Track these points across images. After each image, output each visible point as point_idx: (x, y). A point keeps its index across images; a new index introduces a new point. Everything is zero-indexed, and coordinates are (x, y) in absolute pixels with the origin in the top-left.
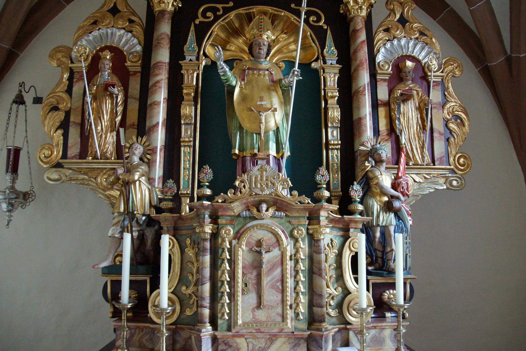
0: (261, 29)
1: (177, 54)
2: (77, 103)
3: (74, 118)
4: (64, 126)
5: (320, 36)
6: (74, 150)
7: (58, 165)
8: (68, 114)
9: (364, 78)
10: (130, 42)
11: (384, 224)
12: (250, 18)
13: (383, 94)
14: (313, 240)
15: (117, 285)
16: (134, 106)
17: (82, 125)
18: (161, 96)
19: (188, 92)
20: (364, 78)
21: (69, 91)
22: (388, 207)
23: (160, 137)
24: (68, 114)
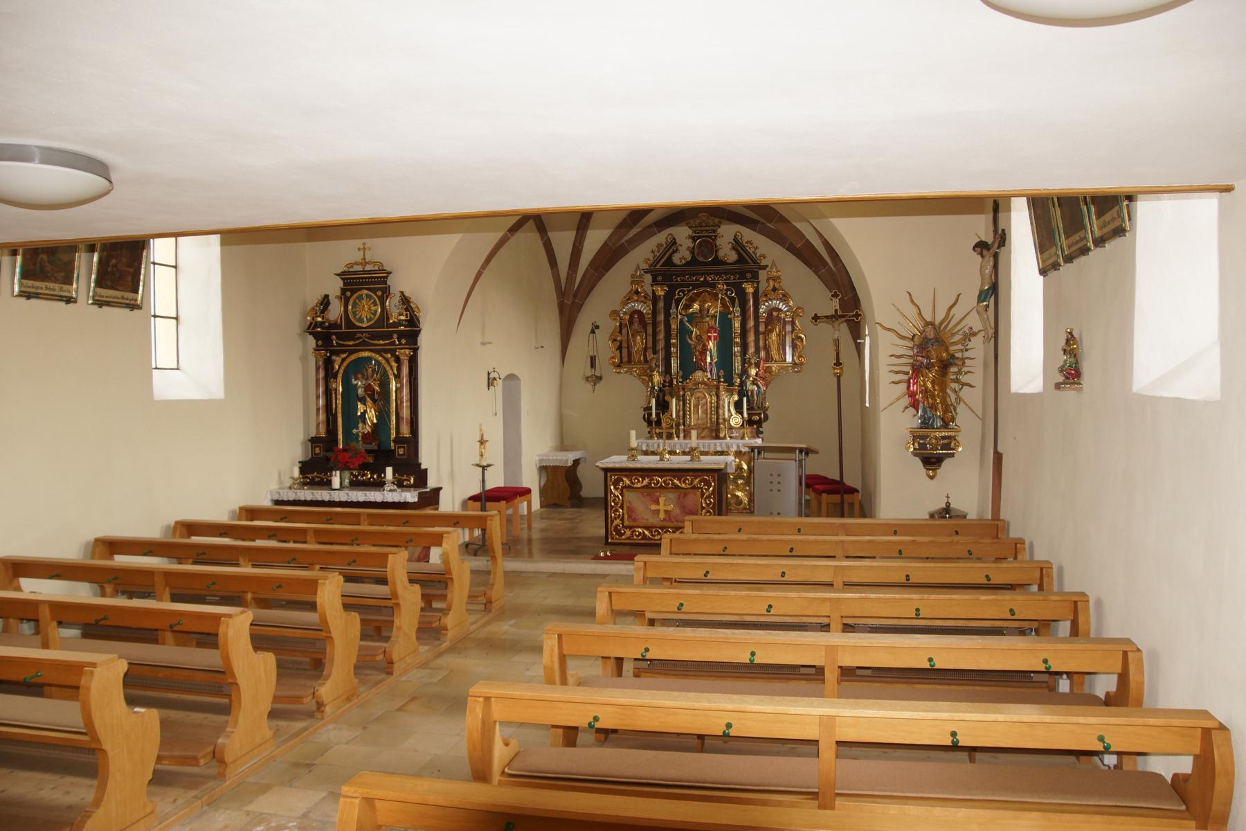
0: (704, 301)
1: (667, 315)
2: (625, 338)
3: (625, 345)
4: (620, 348)
5: (732, 300)
6: (625, 359)
7: (619, 366)
8: (621, 342)
9: (751, 323)
10: (645, 309)
11: (908, 369)
12: (698, 295)
13: (762, 328)
14: (718, 396)
15: (650, 415)
16: (650, 339)
17: (629, 348)
18: (661, 336)
19: (674, 333)
20: (751, 323)
21: (620, 332)
22: (754, 383)
23: (661, 355)
24: (621, 342)
